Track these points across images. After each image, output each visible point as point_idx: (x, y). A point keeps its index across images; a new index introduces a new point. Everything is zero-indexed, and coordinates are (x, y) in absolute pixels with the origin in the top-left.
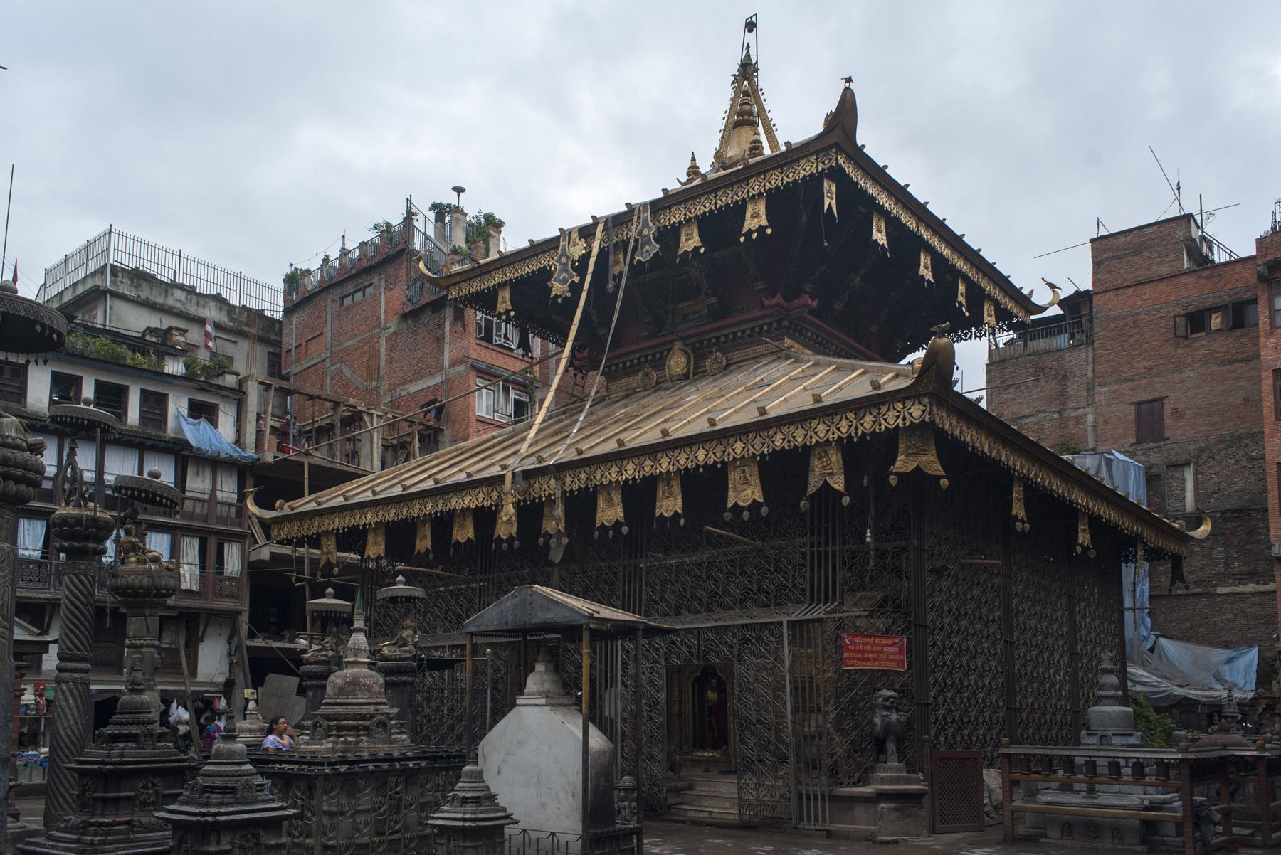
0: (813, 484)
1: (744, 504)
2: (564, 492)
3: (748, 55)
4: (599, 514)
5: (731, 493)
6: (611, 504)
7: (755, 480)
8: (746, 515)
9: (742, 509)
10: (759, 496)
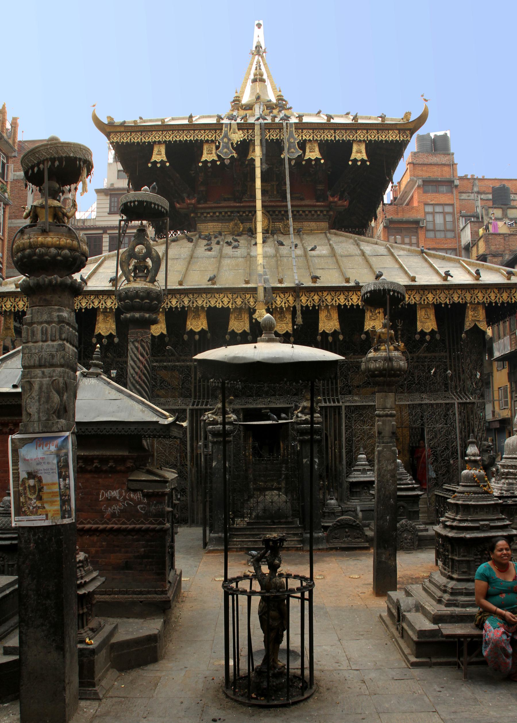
0: (468, 325)
1: (428, 331)
2: (302, 306)
3: (259, 42)
4: (321, 325)
5: (418, 323)
6: (329, 318)
7: (432, 317)
8: (428, 338)
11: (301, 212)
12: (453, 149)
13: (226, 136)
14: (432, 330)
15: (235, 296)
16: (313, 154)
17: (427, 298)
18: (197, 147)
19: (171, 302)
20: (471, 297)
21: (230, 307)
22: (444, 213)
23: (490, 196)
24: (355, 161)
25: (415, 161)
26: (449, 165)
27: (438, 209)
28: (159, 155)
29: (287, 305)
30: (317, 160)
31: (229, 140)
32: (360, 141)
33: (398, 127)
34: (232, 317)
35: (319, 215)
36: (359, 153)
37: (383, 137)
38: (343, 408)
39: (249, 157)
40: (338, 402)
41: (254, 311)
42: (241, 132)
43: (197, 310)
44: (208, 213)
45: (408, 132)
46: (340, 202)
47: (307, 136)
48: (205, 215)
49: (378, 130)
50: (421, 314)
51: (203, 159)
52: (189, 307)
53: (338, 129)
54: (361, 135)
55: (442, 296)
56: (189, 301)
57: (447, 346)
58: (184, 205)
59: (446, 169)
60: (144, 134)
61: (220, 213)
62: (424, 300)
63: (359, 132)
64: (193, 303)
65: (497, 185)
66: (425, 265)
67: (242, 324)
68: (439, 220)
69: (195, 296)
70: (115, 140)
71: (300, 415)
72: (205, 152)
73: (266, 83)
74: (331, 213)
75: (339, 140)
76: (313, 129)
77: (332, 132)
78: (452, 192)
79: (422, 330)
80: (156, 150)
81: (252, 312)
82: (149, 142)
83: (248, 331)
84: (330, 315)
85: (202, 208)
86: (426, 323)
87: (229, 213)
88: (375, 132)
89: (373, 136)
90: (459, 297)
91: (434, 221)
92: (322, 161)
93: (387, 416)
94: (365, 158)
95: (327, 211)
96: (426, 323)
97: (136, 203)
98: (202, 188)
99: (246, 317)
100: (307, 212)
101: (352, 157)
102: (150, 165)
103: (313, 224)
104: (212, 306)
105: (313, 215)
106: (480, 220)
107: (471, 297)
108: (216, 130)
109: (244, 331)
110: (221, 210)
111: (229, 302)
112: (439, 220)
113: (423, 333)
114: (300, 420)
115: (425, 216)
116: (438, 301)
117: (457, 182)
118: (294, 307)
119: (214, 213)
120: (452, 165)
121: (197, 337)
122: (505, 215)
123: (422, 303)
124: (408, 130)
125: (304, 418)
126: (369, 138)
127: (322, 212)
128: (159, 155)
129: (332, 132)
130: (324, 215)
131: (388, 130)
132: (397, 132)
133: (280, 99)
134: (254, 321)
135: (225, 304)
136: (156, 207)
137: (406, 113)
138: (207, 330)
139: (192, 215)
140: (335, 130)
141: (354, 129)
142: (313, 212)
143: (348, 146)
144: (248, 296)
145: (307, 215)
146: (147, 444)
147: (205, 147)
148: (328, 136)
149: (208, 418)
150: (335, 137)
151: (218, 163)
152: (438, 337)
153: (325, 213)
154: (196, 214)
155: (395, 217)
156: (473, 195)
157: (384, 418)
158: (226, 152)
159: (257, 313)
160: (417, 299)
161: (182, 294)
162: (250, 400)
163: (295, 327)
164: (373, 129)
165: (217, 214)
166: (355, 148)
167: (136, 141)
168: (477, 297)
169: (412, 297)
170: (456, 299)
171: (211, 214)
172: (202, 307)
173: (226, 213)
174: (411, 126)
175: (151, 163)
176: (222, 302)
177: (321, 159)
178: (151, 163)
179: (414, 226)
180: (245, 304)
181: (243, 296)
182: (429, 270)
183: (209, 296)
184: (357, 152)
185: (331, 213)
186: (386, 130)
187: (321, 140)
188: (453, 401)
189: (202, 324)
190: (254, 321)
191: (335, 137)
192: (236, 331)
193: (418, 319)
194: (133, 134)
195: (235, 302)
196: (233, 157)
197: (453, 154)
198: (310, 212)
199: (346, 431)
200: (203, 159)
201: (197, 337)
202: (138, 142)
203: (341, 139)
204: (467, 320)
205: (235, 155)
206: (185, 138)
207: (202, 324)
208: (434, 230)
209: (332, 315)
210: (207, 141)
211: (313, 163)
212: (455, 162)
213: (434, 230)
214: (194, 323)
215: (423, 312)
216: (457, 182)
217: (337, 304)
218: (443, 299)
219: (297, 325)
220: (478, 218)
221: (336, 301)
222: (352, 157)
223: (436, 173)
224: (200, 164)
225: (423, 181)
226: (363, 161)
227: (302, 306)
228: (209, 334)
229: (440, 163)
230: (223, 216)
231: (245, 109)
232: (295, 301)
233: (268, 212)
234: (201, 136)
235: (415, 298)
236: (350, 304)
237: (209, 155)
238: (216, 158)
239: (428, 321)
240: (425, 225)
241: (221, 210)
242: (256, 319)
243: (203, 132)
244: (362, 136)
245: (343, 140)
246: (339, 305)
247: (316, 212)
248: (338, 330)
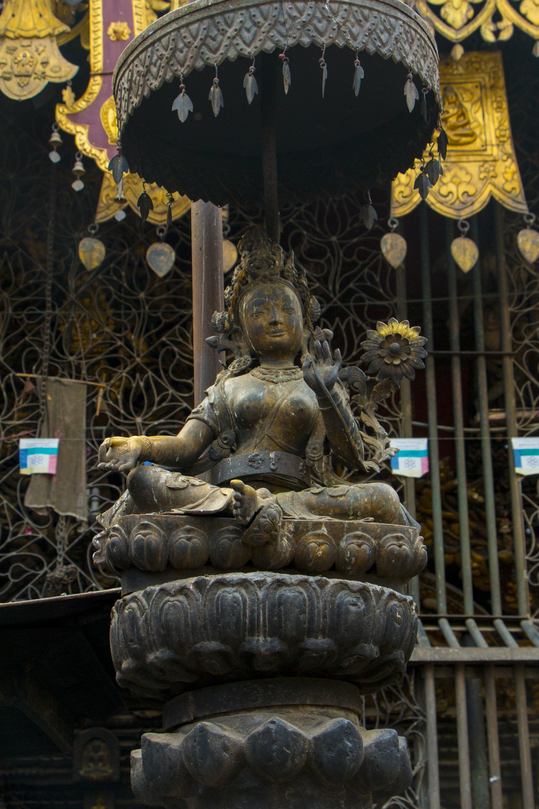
84: (463, 114)
114: (170, 527)
209: (475, 115)
217: (505, 36)
248: (510, 204)
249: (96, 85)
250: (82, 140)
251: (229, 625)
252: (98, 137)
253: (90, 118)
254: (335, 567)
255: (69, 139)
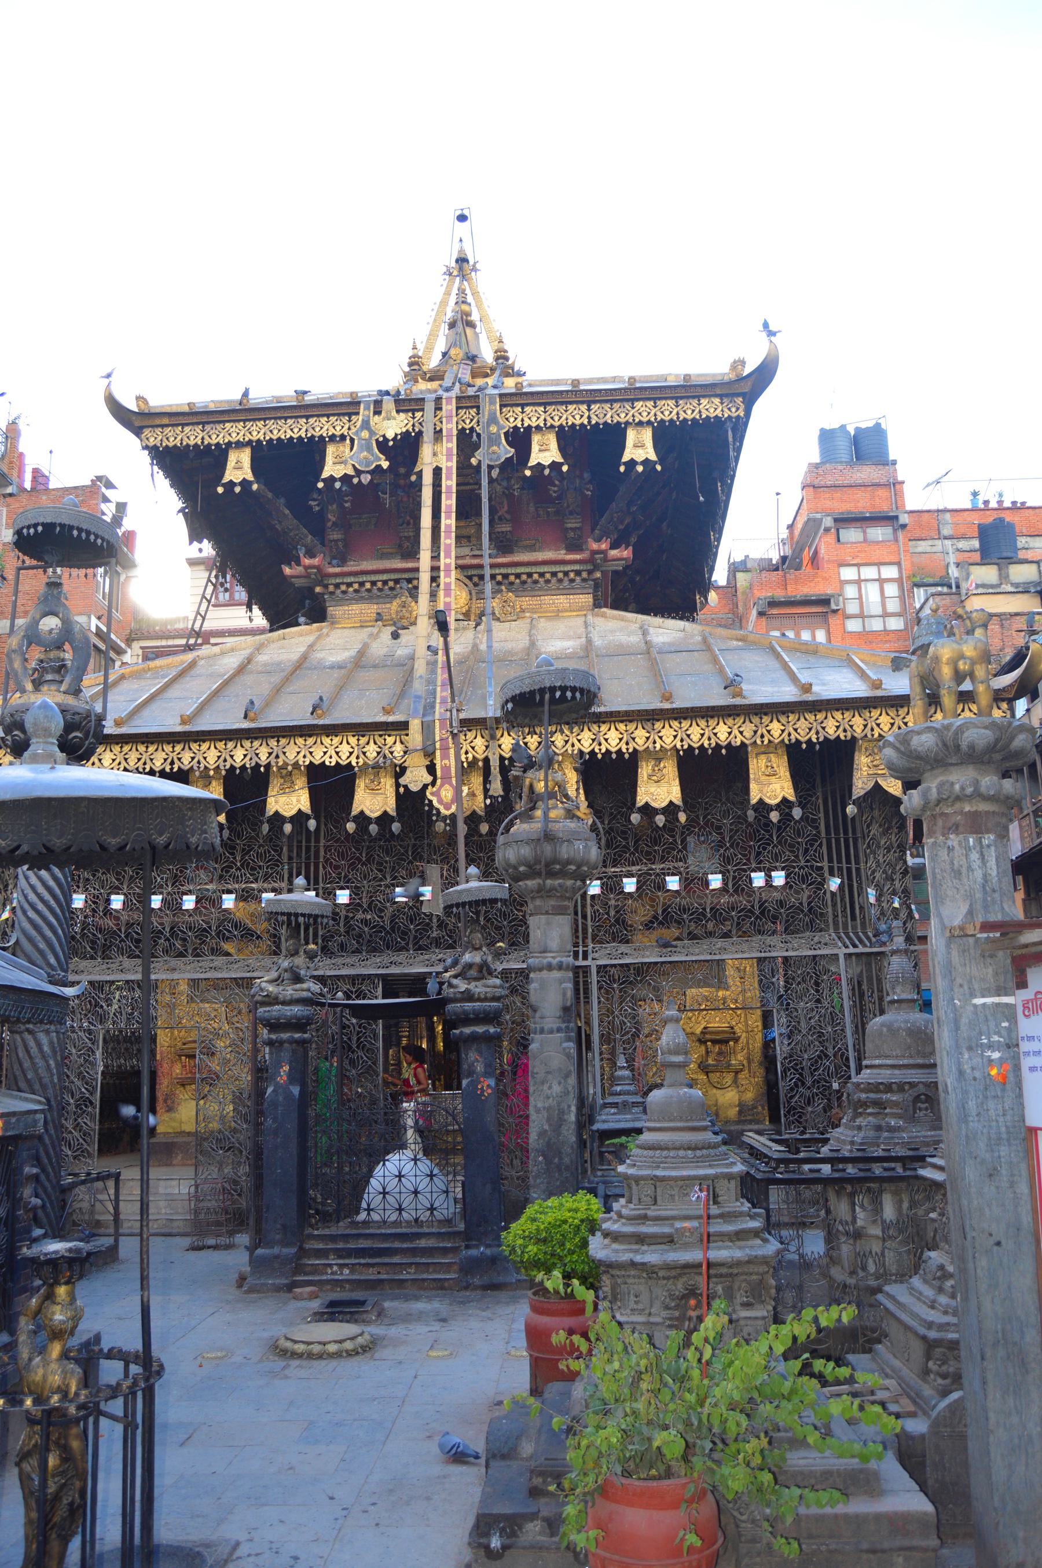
0: (861, 785)
1: (773, 802)
2: (502, 758)
5: (753, 786)
7: (784, 771)
9: (770, 808)
10: (790, 794)
11: (536, 576)
12: (894, 452)
13: (366, 425)
14: (785, 800)
15: (363, 740)
16: (546, 454)
17: (769, 732)
18: (313, 450)
19: (232, 756)
20: (865, 726)
21: (354, 764)
22: (881, 581)
23: (976, 544)
24: (632, 463)
25: (816, 482)
26: (887, 485)
27: (869, 572)
28: (239, 468)
29: (470, 756)
30: (554, 466)
31: (372, 433)
32: (640, 424)
33: (718, 392)
34: (361, 785)
35: (572, 581)
36: (639, 448)
37: (689, 411)
38: (594, 970)
39: (417, 469)
40: (585, 958)
41: (403, 770)
42: (402, 415)
43: (287, 774)
44: (349, 585)
45: (739, 400)
46: (614, 553)
47: (533, 416)
48: (343, 588)
49: (677, 399)
50: (757, 766)
51: (325, 474)
52: (268, 766)
53: (595, 402)
54: (644, 410)
55: (802, 724)
56: (270, 754)
57: (823, 835)
58: (300, 570)
59: (882, 493)
60: (208, 427)
61: (373, 583)
62: (762, 736)
63: (638, 405)
64: (277, 757)
65: (989, 519)
66: (774, 664)
67: (380, 798)
68: (872, 592)
69: (283, 741)
70: (152, 442)
71: (455, 981)
72: (329, 459)
73: (478, 330)
74: (598, 575)
75: (597, 424)
76: (545, 405)
77: (584, 407)
78: (896, 540)
79: (761, 801)
80: (233, 457)
81: (400, 771)
82: (218, 445)
83: (393, 813)
85: (336, 575)
86: (771, 784)
87: (391, 584)
88: (672, 403)
89: (668, 411)
90: (838, 727)
91: (860, 598)
92: (565, 468)
93: (550, 967)
94: (653, 457)
95: (590, 572)
96: (771, 784)
97: (40, 529)
98: (336, 535)
99: (388, 784)
100: (548, 576)
101: (626, 458)
102: (220, 490)
103: (562, 600)
104: (317, 763)
105: (560, 581)
106: (954, 590)
107: (865, 726)
108: (350, 415)
109: (385, 813)
110: (373, 578)
111: (351, 753)
112: (872, 592)
113: (762, 807)
115: (842, 589)
116: (792, 737)
117: (904, 519)
118: (486, 760)
119: (362, 584)
120: (895, 486)
121: (288, 828)
122: (1004, 577)
123: (759, 742)
124: (738, 395)
125: (462, 986)
126: (660, 416)
127: (578, 573)
128: (239, 468)
129: (584, 407)
130: (584, 580)
131: (699, 398)
132: (717, 401)
133: (501, 356)
134: (402, 790)
135: (344, 757)
136: (84, 535)
137: (735, 362)
138: (309, 812)
139: (318, 589)
140: (589, 404)
141: (627, 400)
142: (560, 575)
143: (615, 434)
144: (390, 740)
145: (548, 581)
146: (51, 1043)
147: (331, 450)
148: (576, 416)
149: (262, 990)
150: (589, 417)
151: (355, 481)
152: (797, 813)
153: (585, 575)
154: (326, 586)
155: (780, 594)
156: (939, 543)
157: (545, 974)
158: (366, 458)
159: (408, 772)
160: (748, 734)
161: (256, 738)
162: (401, 957)
163: (488, 801)
164: (666, 398)
165: (368, 586)
166: (631, 435)
167: (192, 443)
168: (878, 725)
169: (736, 732)
170: (831, 731)
171: (356, 586)
172: (296, 765)
173: (385, 582)
174: (746, 388)
175: (223, 485)
176: (337, 753)
177: (562, 464)
178: (223, 485)
179: (820, 609)
180: (385, 757)
181: (380, 741)
182: (782, 674)
183: (310, 741)
184: (635, 446)
185: (598, 575)
186: (694, 397)
187: (561, 427)
188: (835, 951)
189: (298, 801)
190: (402, 790)
191: (589, 417)
192: (367, 813)
193: (752, 776)
194: (187, 429)
195: (364, 753)
196: (379, 467)
197: (894, 463)
198: (554, 574)
199: (601, 1021)
200: (325, 474)
201: (288, 828)
202: (196, 445)
203: (601, 421)
204: (856, 775)
205: (385, 465)
206: (289, 434)
207: (298, 801)
208: (862, 616)
210: (332, 438)
211: (547, 472)
212: (900, 479)
213: (862, 616)
214: (283, 799)
215: (763, 761)
216: (904, 519)
218: (802, 729)
219: (491, 797)
220: (950, 587)
221: (573, 745)
222: (626, 458)
223: (861, 503)
224: (320, 485)
225: (836, 520)
226: (646, 462)
227: (502, 758)
228: (312, 824)
229: (867, 482)
230: (380, 590)
231: (431, 379)
232: (487, 747)
233: (470, 578)
234: (322, 427)
235: (741, 733)
236: (603, 750)
237: (338, 467)
238: (351, 472)
239: (773, 779)
240: (841, 606)
241: (373, 578)
242: (406, 787)
243: (324, 420)
244: (645, 414)
245: (605, 423)
246: (581, 752)
247: (566, 574)
249: (439, 782)
250: (435, 803)
251: (465, 1013)
252: (440, 801)
253: (436, 794)
254: (485, 999)
255: (431, 801)
